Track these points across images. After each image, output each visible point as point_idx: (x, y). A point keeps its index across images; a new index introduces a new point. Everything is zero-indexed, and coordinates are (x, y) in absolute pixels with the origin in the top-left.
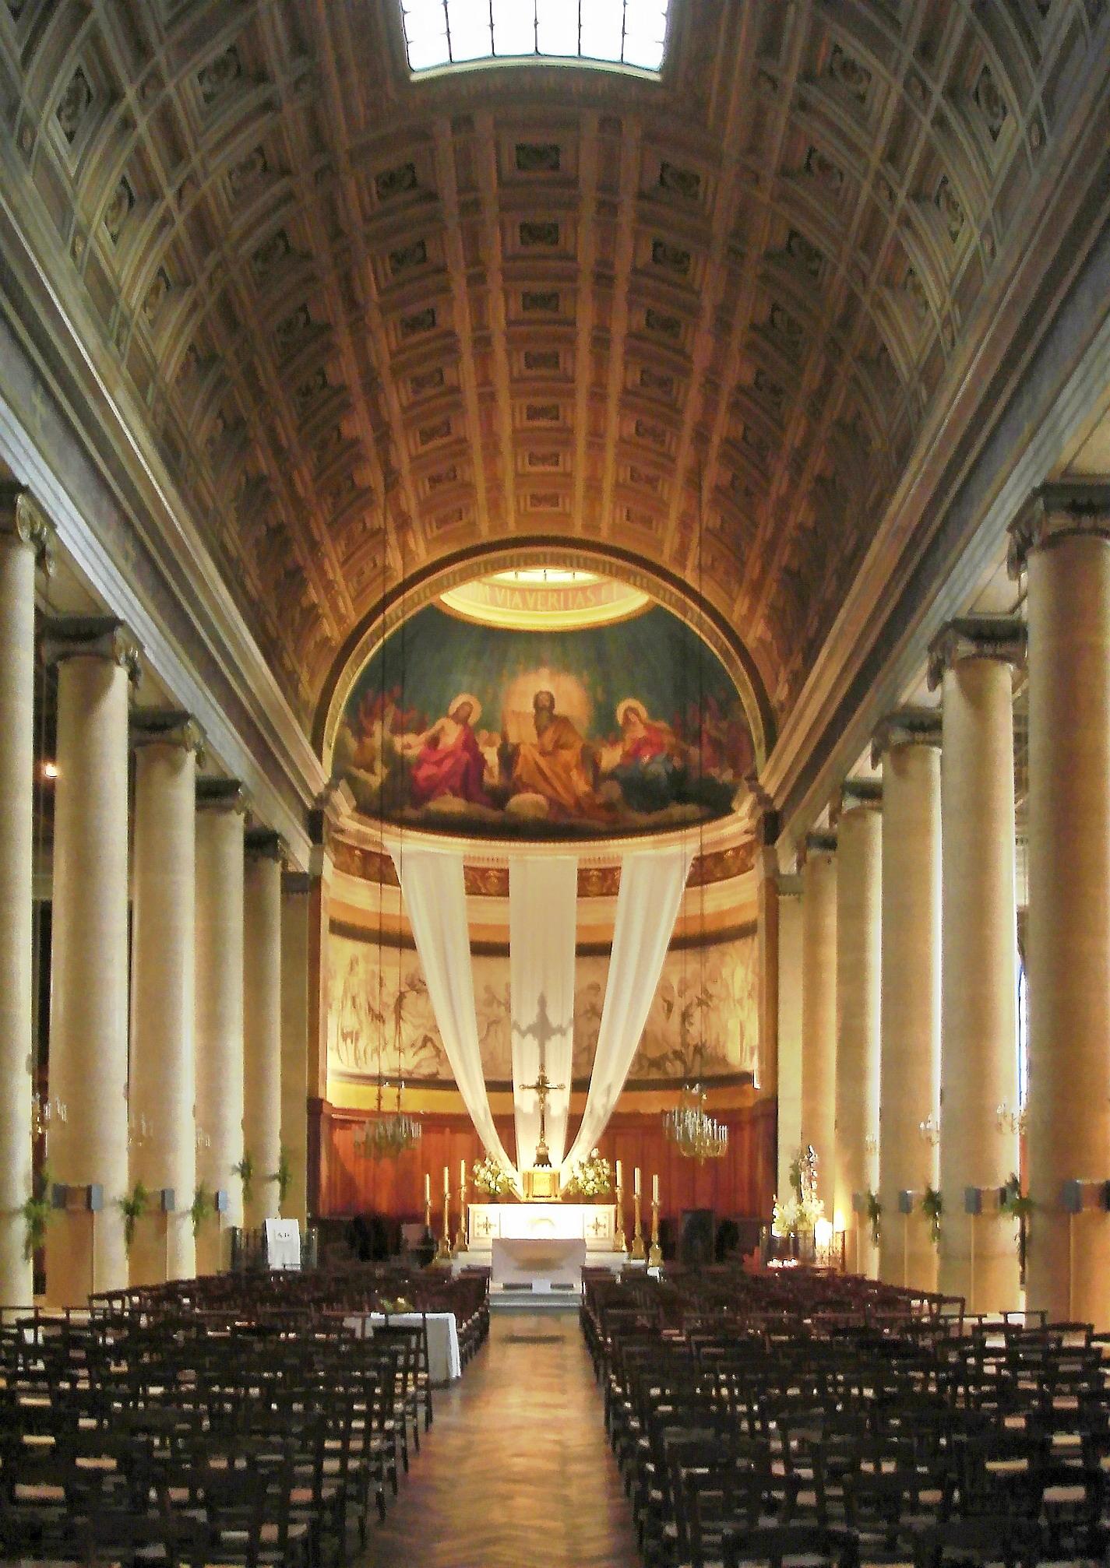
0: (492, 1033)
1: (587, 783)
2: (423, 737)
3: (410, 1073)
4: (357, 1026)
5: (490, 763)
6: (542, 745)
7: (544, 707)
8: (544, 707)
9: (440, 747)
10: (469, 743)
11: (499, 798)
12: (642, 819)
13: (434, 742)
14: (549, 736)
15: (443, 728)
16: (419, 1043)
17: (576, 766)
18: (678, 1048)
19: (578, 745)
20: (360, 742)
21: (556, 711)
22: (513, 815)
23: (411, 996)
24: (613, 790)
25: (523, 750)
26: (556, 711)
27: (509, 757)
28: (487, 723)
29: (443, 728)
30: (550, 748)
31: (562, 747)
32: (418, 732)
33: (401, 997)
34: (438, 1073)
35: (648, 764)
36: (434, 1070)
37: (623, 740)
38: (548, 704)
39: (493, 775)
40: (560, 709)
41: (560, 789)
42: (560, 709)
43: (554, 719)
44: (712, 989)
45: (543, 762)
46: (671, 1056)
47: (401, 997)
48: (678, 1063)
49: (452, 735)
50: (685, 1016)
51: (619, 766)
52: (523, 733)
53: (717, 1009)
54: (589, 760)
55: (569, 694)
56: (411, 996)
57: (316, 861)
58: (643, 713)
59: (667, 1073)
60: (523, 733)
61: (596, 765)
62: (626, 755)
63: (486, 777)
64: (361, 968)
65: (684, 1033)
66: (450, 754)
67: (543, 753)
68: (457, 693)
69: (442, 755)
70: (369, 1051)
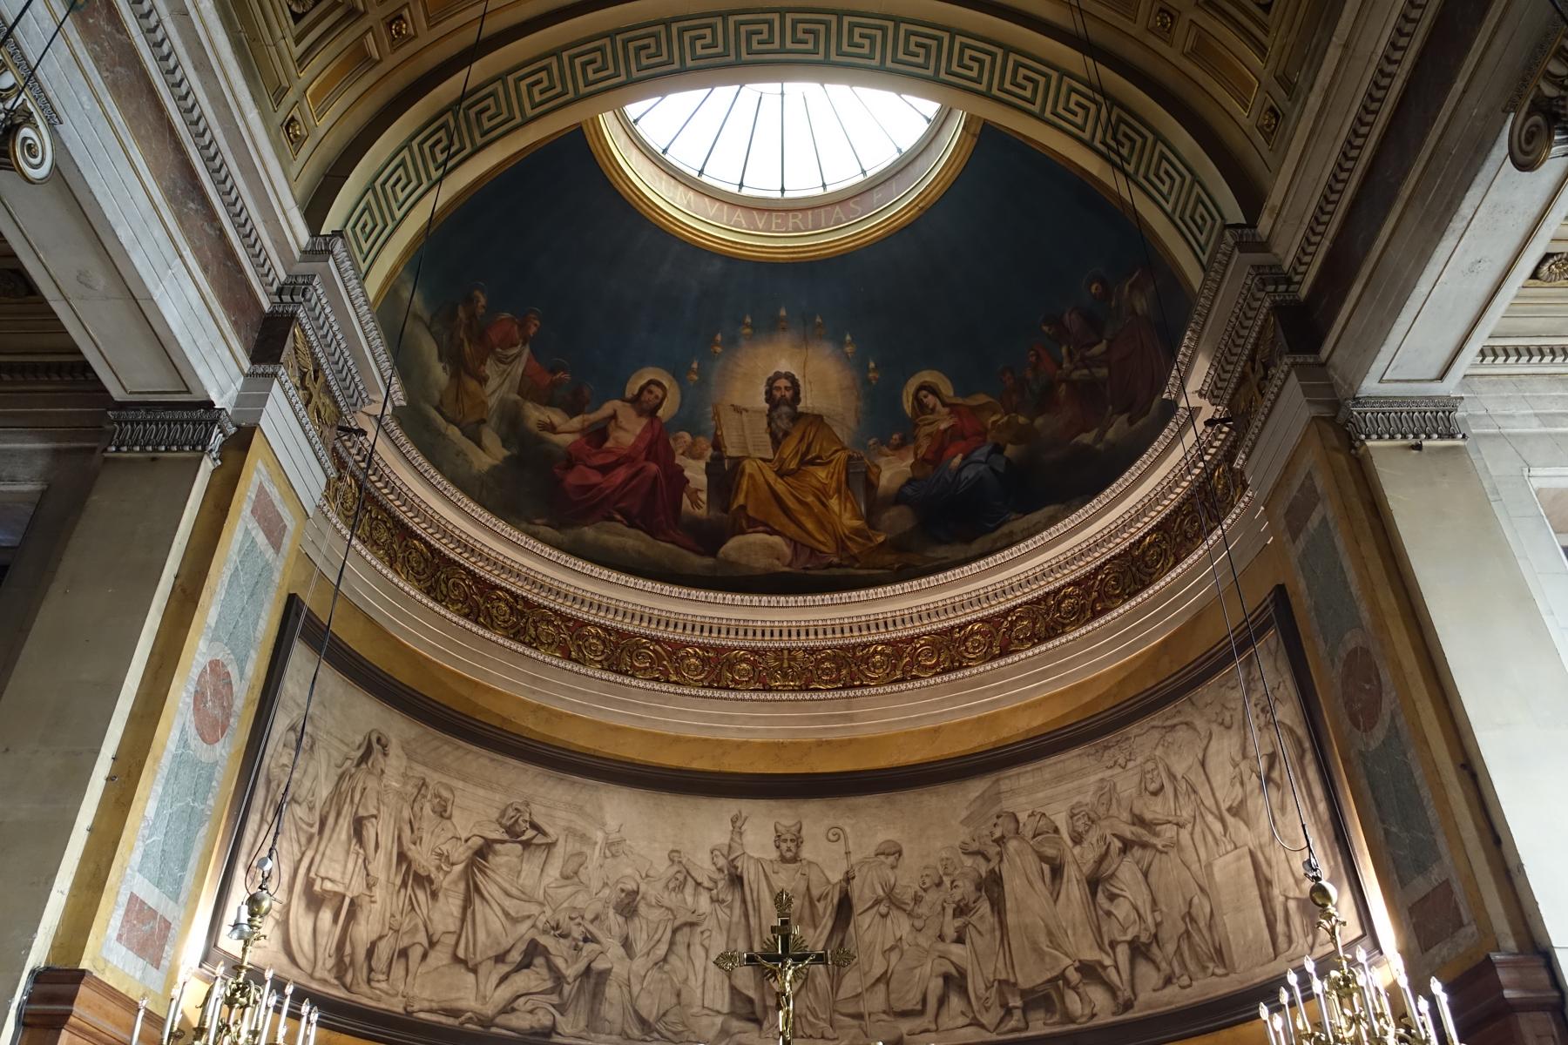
0: (681, 949)
1: (856, 516)
2: (576, 422)
3: (486, 1022)
4: (357, 887)
5: (692, 485)
6: (782, 461)
7: (783, 398)
8: (783, 398)
9: (609, 444)
10: (657, 445)
11: (709, 538)
12: (959, 551)
13: (598, 435)
14: (789, 448)
15: (614, 417)
16: (515, 956)
17: (838, 491)
18: (1091, 954)
19: (842, 455)
20: (455, 376)
21: (801, 407)
22: (732, 564)
23: (507, 855)
24: (898, 520)
25: (749, 467)
26: (801, 407)
27: (724, 475)
28: (689, 420)
29: (614, 417)
30: (793, 466)
31: (812, 462)
32: (572, 411)
33: (484, 851)
34: (553, 1030)
35: (960, 469)
36: (547, 1021)
37: (915, 438)
38: (788, 394)
39: (697, 505)
40: (809, 401)
41: (810, 526)
42: (809, 401)
43: (797, 417)
44: (1155, 809)
45: (780, 487)
46: (1074, 976)
47: (484, 851)
48: (1098, 995)
49: (629, 431)
50: (1094, 883)
51: (909, 482)
52: (747, 438)
53: (1176, 844)
54: (859, 479)
55: (823, 377)
56: (507, 855)
57: (253, 400)
58: (947, 389)
59: (1069, 1018)
60: (747, 438)
61: (870, 486)
62: (920, 462)
63: (686, 501)
64: (394, 763)
65: (1097, 922)
66: (626, 459)
67: (781, 474)
68: (643, 363)
69: (611, 459)
70: (384, 950)
